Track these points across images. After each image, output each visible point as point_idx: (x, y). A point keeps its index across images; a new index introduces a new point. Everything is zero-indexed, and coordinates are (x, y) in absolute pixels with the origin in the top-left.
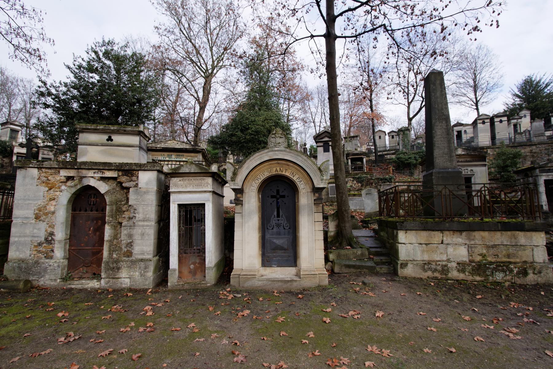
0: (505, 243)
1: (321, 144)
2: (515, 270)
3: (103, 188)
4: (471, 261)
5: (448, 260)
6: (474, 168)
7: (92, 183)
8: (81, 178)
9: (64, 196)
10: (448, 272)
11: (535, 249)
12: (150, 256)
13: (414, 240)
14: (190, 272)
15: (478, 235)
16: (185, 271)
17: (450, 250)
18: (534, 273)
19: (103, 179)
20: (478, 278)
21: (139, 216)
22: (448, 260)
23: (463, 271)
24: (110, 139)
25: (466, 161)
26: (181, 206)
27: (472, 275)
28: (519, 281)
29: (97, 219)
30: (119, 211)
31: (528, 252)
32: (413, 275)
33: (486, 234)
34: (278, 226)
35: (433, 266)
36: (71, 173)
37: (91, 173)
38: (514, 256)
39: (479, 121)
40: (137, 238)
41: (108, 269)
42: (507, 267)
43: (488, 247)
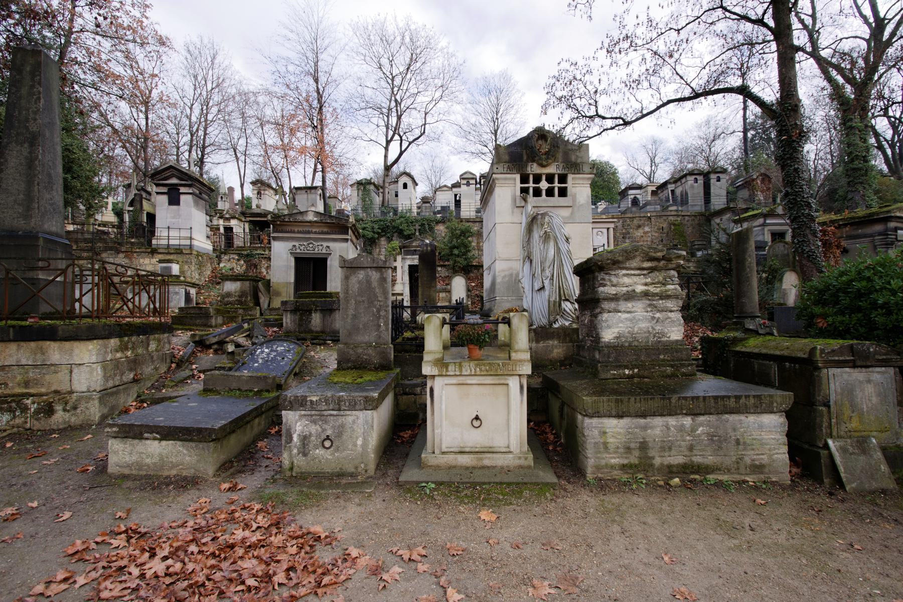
0: (24, 362)
1: (165, 190)
2: (33, 408)
6: (332, 245)
11: (75, 370)
18: (65, 410)
25: (322, 233)
28: (37, 425)
31: (63, 375)
38: (37, 382)
42: (19, 403)
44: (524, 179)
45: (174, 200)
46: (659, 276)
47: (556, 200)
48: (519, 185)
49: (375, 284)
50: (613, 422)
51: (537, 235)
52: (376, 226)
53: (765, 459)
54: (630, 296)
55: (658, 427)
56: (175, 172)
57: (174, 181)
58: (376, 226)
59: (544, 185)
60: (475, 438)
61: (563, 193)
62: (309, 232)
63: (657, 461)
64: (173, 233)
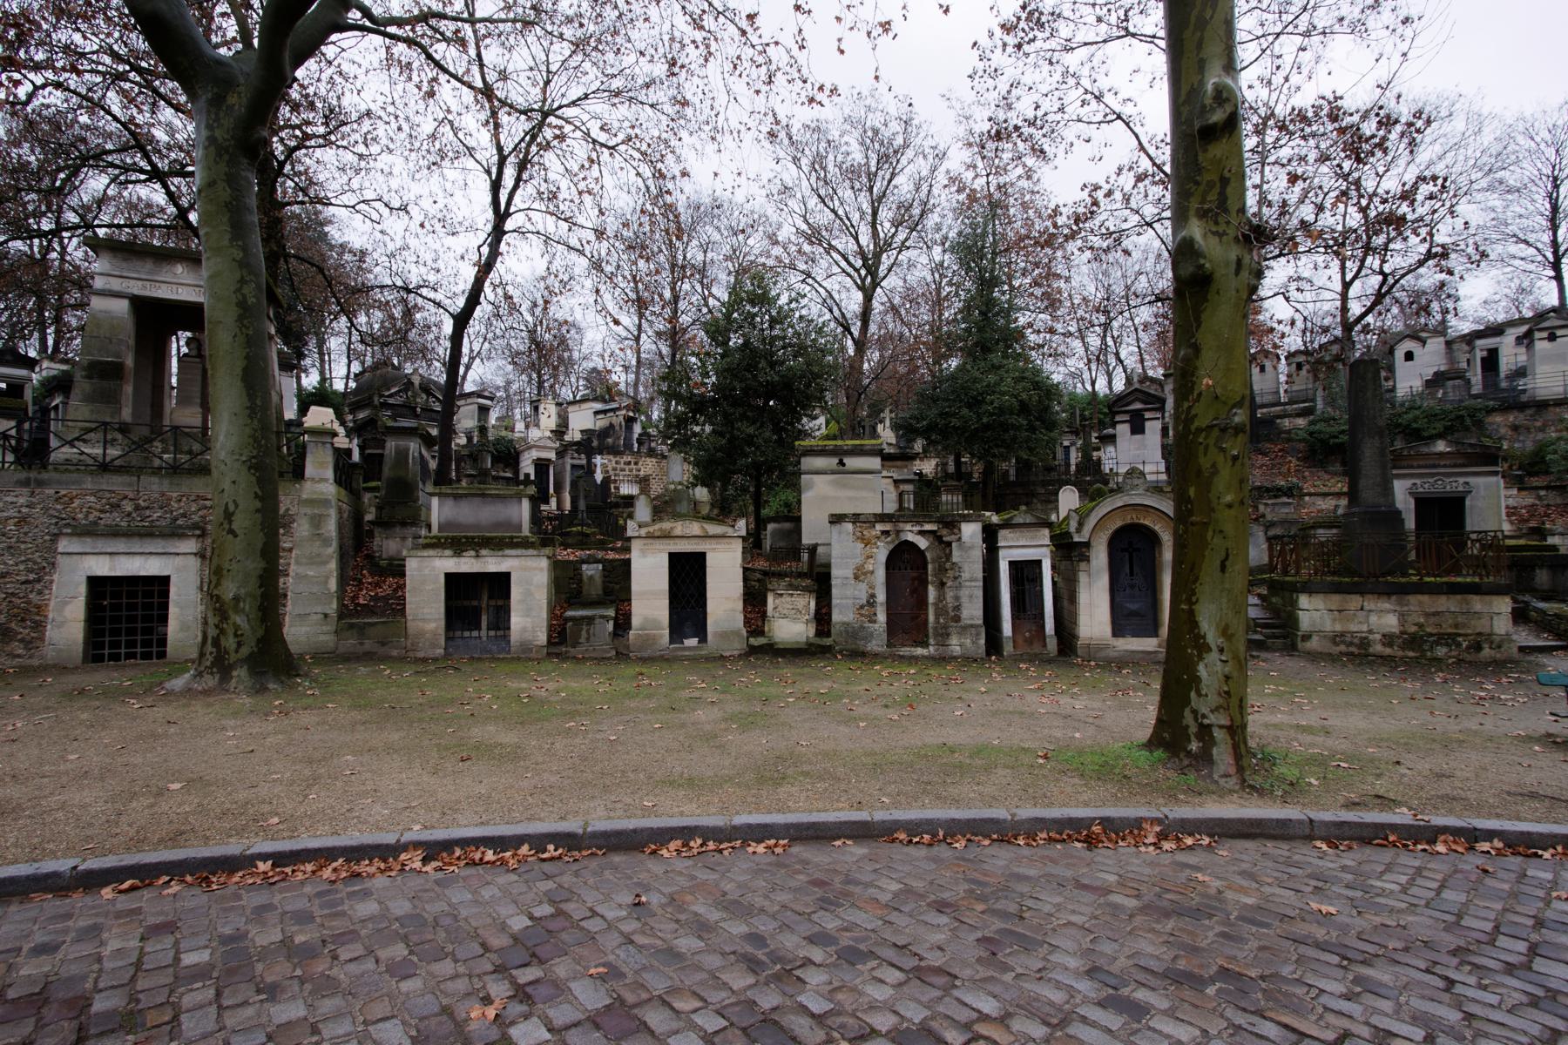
1: (1126, 417)
2: (1465, 644)
3: (922, 543)
4: (1402, 633)
5: (1370, 631)
6: (1472, 480)
7: (910, 537)
8: (898, 532)
9: (882, 553)
12: (981, 622)
13: (1321, 606)
14: (1026, 640)
15: (1414, 599)
16: (1020, 641)
17: (1373, 619)
19: (921, 533)
20: (1411, 654)
21: (965, 575)
22: (1370, 631)
23: (1390, 645)
24: (841, 463)
25: (1455, 466)
26: (1013, 565)
27: (1403, 649)
29: (914, 579)
30: (942, 570)
31: (1485, 622)
33: (1425, 598)
34: (1132, 587)
35: (1348, 639)
36: (887, 527)
37: (908, 527)
38: (1464, 626)
39: (1537, 335)
40: (964, 600)
41: (936, 635)
43: (1427, 615)
56: (1140, 396)
62: (1434, 466)
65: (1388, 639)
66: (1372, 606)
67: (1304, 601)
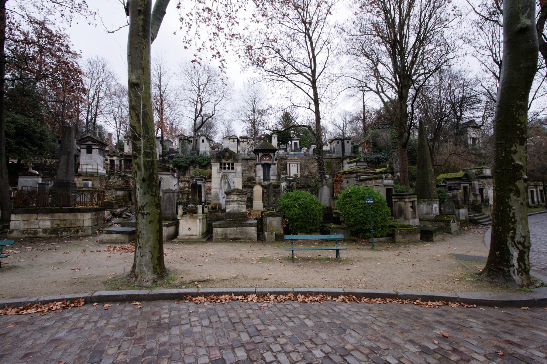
1: (85, 147)
4: (51, 228)
5: (39, 228)
6: (163, 176)
10: (37, 233)
15: (57, 215)
17: (41, 223)
20: (53, 236)
23: (46, 233)
27: (50, 234)
28: (74, 235)
31: (81, 222)
32: (16, 236)
33: (61, 214)
38: (74, 224)
42: (69, 229)
43: (61, 220)
44: (221, 164)
45: (89, 151)
46: (241, 196)
47: (231, 170)
48: (219, 166)
49: (171, 197)
50: (219, 229)
51: (223, 181)
52: (188, 161)
53: (252, 236)
54: (233, 201)
55: (229, 230)
56: (90, 139)
57: (90, 143)
58: (188, 161)
59: (227, 166)
60: (189, 233)
61: (233, 168)
63: (228, 237)
64: (89, 167)
65: (45, 231)
66: (41, 218)
67: (13, 217)
